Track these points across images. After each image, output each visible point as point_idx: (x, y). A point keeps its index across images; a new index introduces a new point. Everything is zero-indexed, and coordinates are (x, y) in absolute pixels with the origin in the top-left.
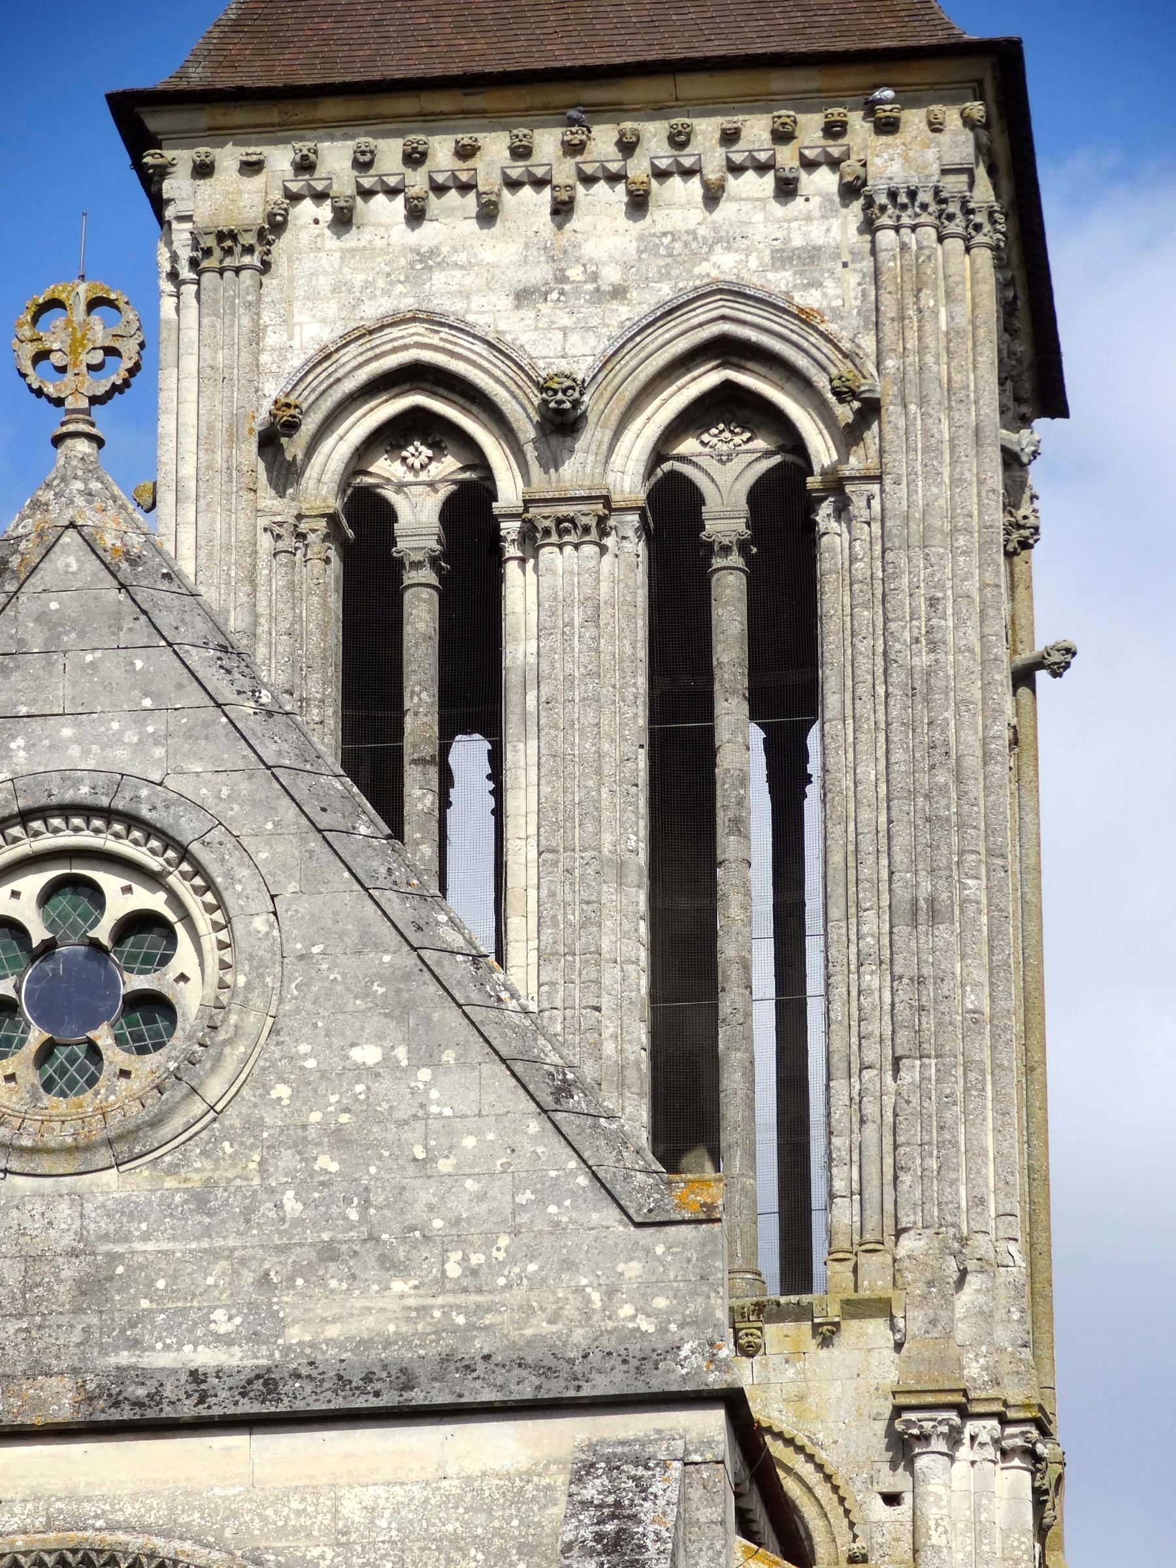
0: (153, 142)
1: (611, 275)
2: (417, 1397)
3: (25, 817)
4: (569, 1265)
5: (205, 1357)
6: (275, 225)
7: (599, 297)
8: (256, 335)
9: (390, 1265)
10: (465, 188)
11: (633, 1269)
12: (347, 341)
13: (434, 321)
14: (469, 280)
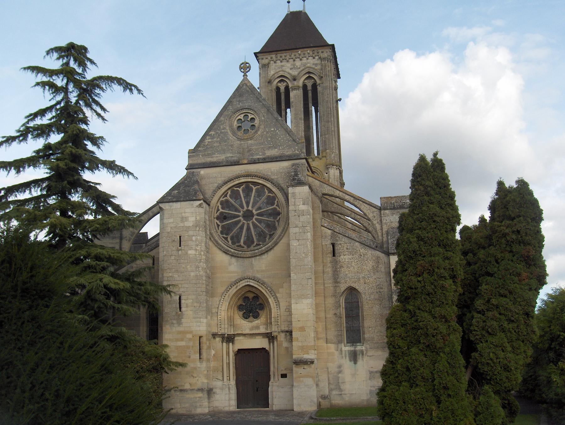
0: (258, 57)
1: (299, 67)
2: (278, 159)
3: (241, 109)
4: (291, 147)
5: (258, 157)
6: (269, 63)
7: (297, 69)
8: (268, 73)
9: (276, 148)
11: (297, 147)
14: (286, 68)
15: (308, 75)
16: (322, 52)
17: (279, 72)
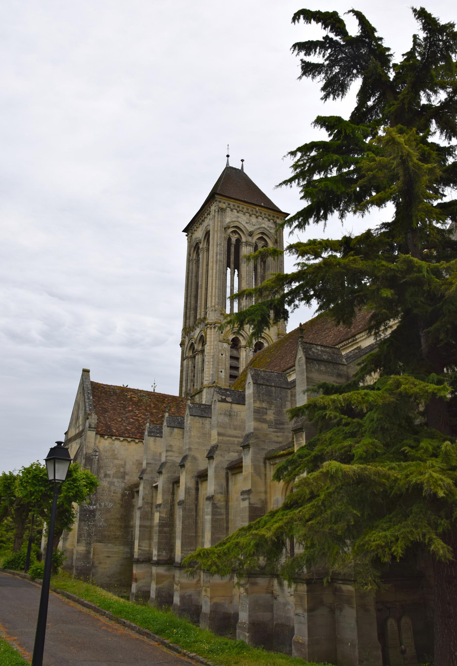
1: (254, 223)
10: (242, 211)
12: (232, 222)
13: (240, 223)
15: (261, 236)
16: (278, 218)
17: (235, 221)
